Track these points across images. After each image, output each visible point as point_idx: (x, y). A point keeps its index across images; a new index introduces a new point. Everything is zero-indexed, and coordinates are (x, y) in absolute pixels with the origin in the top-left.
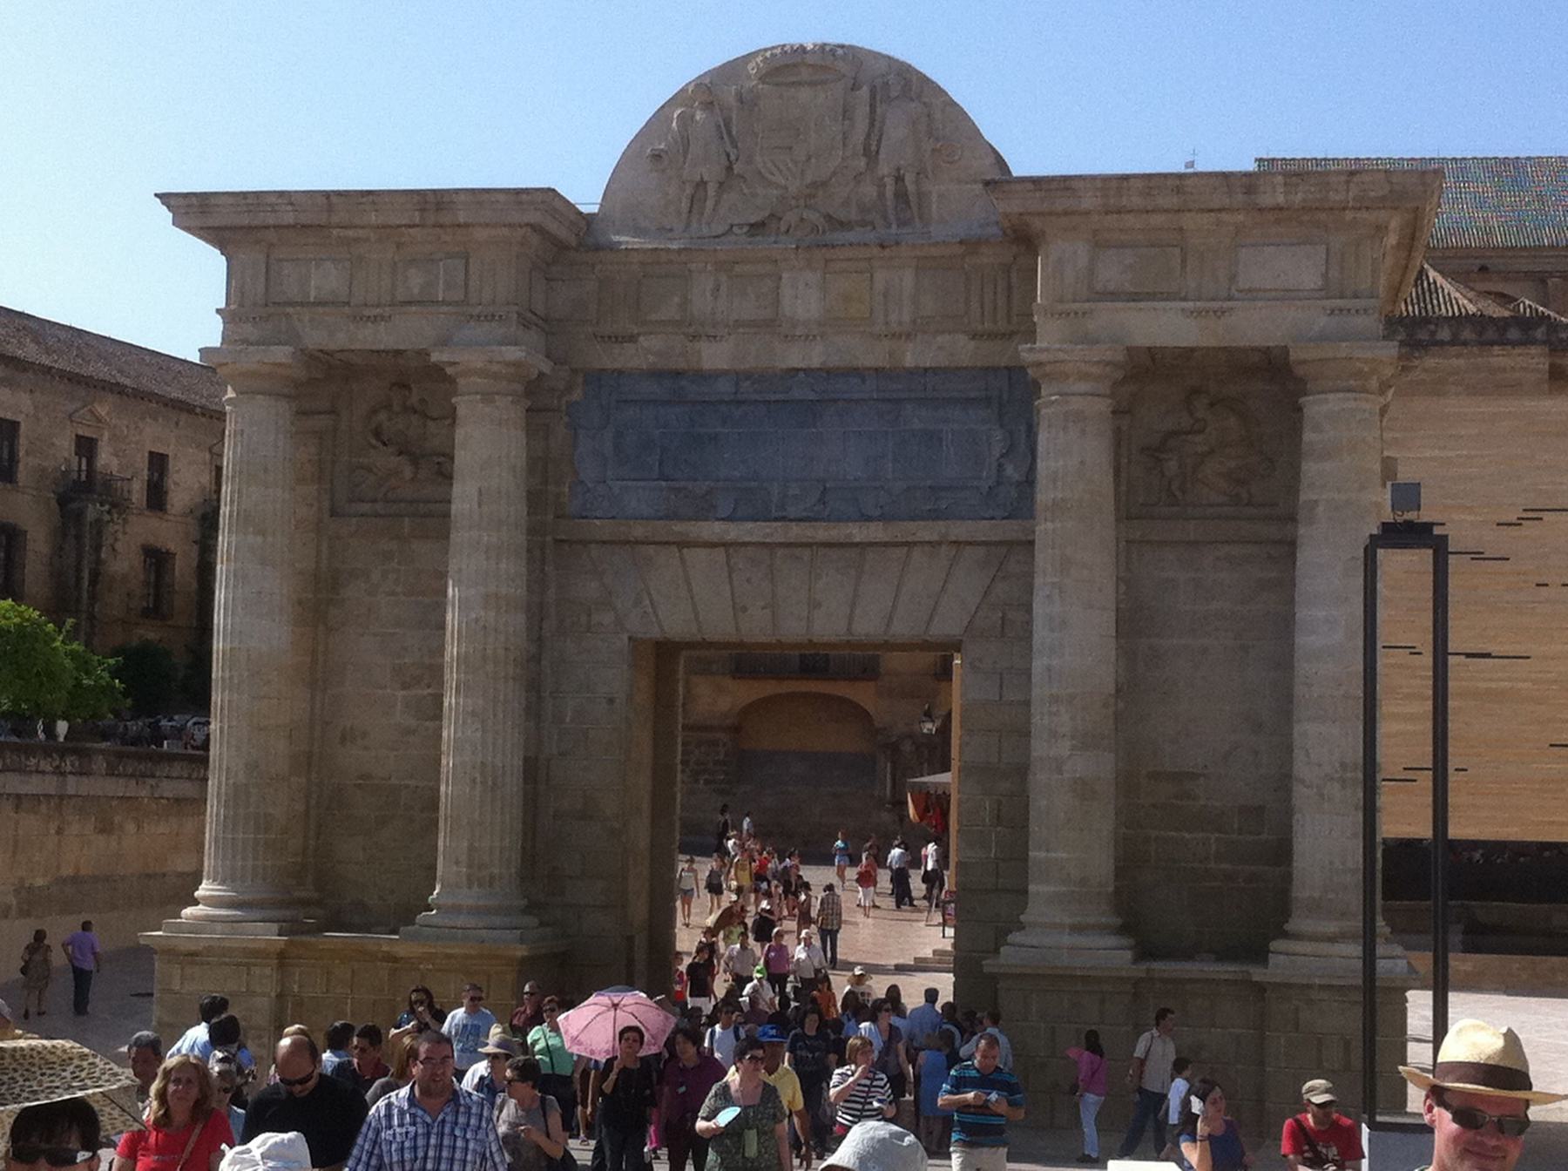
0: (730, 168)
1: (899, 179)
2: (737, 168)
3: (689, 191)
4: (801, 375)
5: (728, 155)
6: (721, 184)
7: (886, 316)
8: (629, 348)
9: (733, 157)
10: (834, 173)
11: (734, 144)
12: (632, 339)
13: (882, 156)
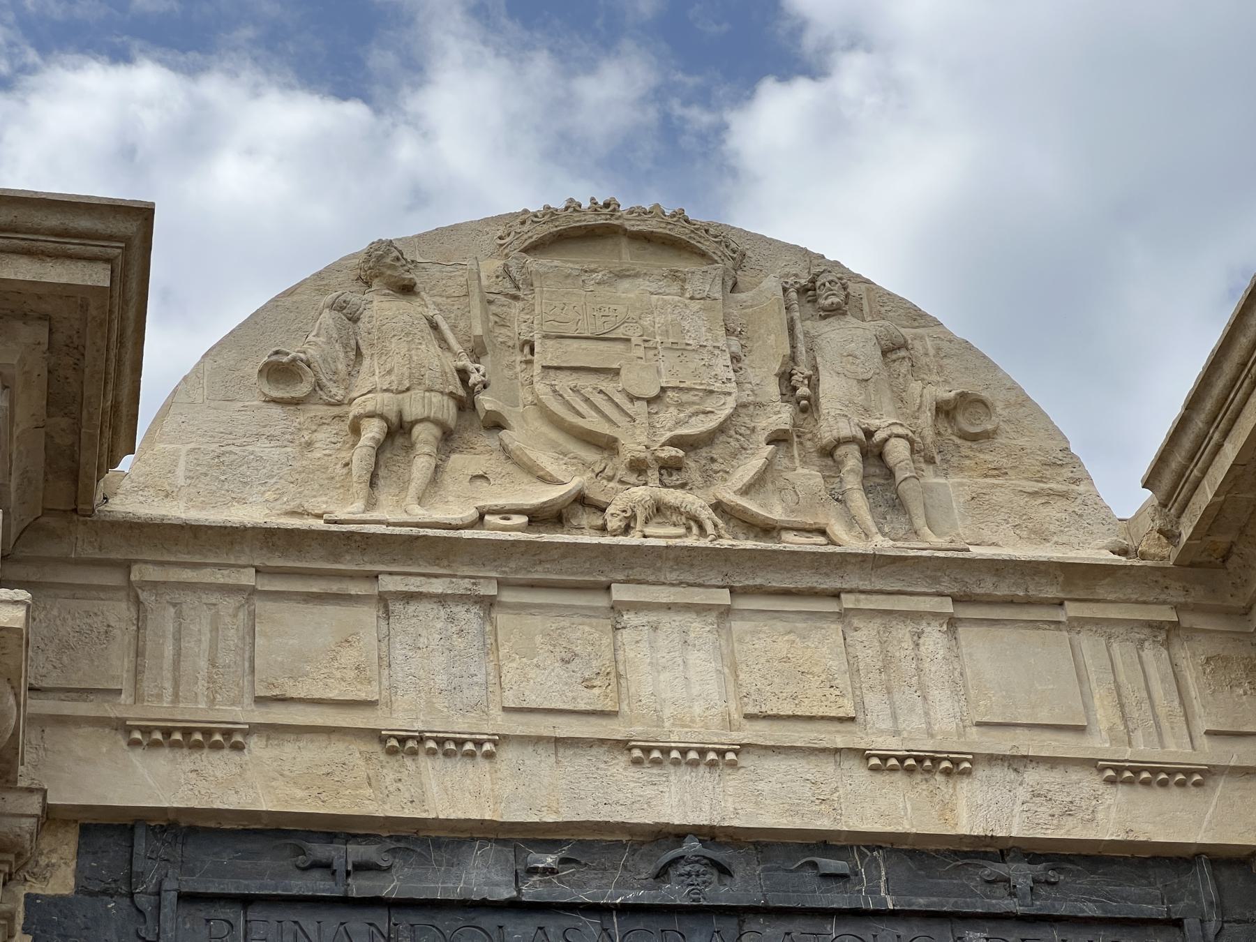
0: (465, 405)
1: (873, 452)
2: (486, 402)
3: (373, 431)
4: (692, 846)
5: (463, 374)
6: (448, 438)
7: (894, 717)
8: (218, 764)
9: (474, 378)
10: (722, 429)
11: (477, 352)
12: (227, 738)
13: (828, 405)
